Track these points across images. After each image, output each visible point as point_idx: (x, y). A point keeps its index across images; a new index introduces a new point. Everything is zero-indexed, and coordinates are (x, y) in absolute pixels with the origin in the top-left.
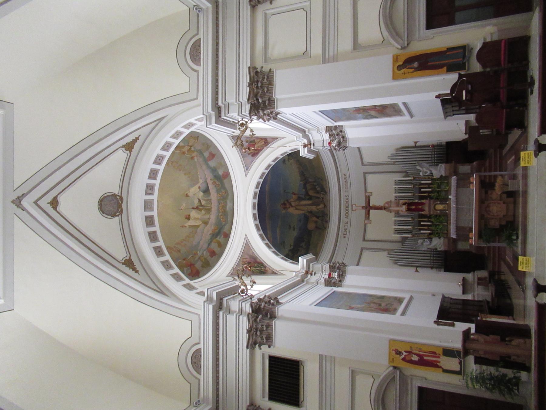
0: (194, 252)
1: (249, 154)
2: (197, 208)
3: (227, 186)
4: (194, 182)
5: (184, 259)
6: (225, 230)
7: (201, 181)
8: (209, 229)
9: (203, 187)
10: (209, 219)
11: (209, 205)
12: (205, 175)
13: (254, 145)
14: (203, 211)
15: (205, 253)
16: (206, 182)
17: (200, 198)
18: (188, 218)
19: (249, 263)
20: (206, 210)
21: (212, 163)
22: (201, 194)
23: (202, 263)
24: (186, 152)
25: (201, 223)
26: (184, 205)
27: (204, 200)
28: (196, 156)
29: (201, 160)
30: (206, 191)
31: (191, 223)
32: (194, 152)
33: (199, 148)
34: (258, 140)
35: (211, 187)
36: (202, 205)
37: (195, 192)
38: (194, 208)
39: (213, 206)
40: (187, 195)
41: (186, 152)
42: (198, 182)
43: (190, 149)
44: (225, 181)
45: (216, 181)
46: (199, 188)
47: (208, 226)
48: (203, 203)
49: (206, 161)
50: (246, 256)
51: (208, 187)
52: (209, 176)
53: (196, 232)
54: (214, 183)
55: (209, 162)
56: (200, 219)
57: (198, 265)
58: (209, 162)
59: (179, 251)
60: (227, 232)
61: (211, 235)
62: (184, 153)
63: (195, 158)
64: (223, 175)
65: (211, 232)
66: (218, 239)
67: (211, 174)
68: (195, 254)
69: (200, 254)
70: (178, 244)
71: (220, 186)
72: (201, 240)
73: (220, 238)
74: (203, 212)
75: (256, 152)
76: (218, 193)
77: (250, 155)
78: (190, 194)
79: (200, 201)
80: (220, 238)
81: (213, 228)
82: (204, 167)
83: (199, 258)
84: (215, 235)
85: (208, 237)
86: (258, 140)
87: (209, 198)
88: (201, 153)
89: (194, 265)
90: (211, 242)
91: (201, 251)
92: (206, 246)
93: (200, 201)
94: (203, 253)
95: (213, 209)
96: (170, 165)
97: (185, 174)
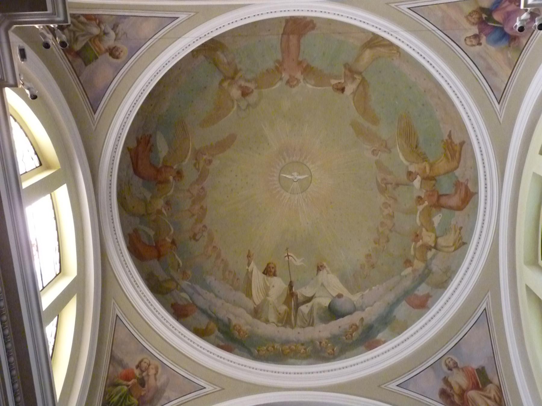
0: (189, 272)
1: (446, 381)
2: (291, 294)
3: (348, 353)
4: (354, 281)
5: (173, 242)
7: (356, 298)
8: (242, 320)
9: (342, 305)
10: (267, 321)
11: (299, 322)
12: (370, 303)
13: (476, 387)
14: (284, 308)
15: (184, 295)
16: (355, 309)
17: (315, 301)
18: (269, 271)
19: (142, 383)
20: (289, 315)
21: (402, 310)
22: (326, 302)
23: (161, 279)
24: (420, 243)
25: (258, 302)
28: (414, 271)
29: (407, 283)
30: (333, 313)
31: (258, 279)
32: (424, 260)
33: (436, 266)
34: (493, 394)
35: (344, 322)
36: (298, 305)
37: (328, 287)
38: (291, 286)
39: (298, 330)
40: (320, 268)
41: (420, 243)
42: (352, 291)
43: (429, 248)
44: (362, 348)
45: (360, 331)
46: (340, 296)
47: (249, 318)
48: (305, 309)
49: (406, 295)
50: (162, 379)
51: (343, 316)
52: (370, 314)
53: (236, 289)
55: (404, 303)
57: (154, 265)
58: (404, 303)
59: (194, 237)
61: (226, 320)
62: (417, 237)
63: (409, 270)
65: (234, 321)
66: (217, 332)
67: (374, 318)
68: (184, 273)
69: (184, 284)
70: (211, 239)
72: (216, 296)
73: (217, 337)
74: (283, 308)
75: (456, 399)
76: (328, 339)
77: (441, 385)
80: (217, 337)
81: (245, 328)
82: (391, 297)
83: (173, 279)
85: (222, 314)
86: (493, 394)
87: (315, 321)
88: (424, 276)
89: (159, 256)
90: (210, 317)
91: (190, 290)
92: (200, 302)
93: (309, 300)
94: (183, 290)
96: (386, 212)
97: (368, 256)
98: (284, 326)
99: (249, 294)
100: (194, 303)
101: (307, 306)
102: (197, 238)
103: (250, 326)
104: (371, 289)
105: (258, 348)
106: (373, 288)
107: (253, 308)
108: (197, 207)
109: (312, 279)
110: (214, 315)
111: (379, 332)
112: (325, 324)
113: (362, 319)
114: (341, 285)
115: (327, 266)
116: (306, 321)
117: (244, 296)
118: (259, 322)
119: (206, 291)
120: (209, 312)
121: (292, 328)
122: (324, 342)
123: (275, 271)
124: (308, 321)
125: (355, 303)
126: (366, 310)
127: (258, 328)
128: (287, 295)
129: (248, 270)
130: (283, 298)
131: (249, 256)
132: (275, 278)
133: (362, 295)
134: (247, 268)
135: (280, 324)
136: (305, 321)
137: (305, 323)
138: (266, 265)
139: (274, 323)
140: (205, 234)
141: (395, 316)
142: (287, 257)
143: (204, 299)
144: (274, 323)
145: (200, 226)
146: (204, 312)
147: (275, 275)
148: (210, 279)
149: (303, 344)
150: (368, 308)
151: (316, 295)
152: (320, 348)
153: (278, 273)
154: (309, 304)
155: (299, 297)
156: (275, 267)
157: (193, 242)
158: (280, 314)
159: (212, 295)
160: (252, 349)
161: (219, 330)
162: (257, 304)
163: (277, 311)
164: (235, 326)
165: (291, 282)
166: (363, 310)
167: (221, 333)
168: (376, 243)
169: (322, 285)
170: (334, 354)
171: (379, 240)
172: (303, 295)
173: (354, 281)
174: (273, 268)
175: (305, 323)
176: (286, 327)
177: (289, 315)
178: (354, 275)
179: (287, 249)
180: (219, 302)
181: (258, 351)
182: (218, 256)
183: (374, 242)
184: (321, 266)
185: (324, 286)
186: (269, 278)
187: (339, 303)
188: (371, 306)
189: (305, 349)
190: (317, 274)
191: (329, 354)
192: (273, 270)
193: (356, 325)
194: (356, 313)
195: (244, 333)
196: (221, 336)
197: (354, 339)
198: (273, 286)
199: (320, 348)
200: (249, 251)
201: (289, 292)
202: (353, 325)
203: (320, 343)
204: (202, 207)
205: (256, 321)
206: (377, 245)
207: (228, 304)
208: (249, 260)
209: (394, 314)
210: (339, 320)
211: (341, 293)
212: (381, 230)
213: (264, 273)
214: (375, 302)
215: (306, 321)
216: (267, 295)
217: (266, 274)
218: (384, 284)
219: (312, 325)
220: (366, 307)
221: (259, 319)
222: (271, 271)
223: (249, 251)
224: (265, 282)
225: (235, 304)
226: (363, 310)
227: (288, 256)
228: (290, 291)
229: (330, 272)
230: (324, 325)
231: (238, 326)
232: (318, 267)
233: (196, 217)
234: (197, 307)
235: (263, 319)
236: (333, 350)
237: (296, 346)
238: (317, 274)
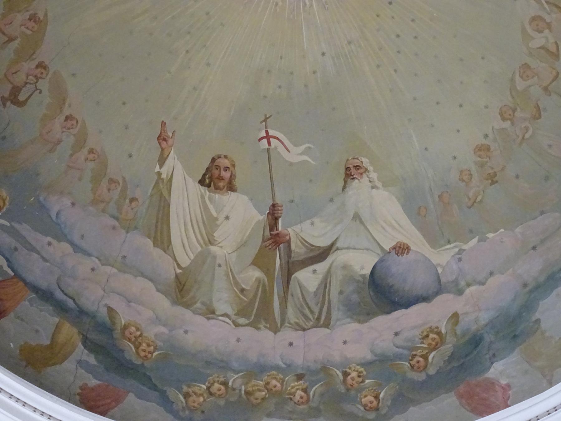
2: (275, 239)
4: (439, 210)
6: (131, 397)
7: (442, 258)
9: (407, 275)
10: (210, 313)
11: (292, 315)
14: (256, 274)
17: (337, 258)
18: (215, 178)
22: (363, 263)
25: (185, 261)
26: (295, 154)
27: (325, 284)
30: (382, 293)
31: (186, 197)
36: (290, 268)
37: (373, 224)
38: (274, 215)
39: (288, 334)
40: (351, 172)
42: (434, 243)
45: (447, 348)
46: (401, 249)
47: (164, 303)
48: (308, 278)
51: (407, 304)
52: (476, 306)
53: (129, 227)
54: (434, 337)
56: (203, 258)
60: (110, 413)
64: (491, 385)
66: (81, 352)
67: (485, 317)
70: (60, 97)
71: (421, 377)
72: (77, 248)
73: (80, 362)
76: (366, 364)
78: (359, 188)
79: (322, 254)
81: (152, 332)
82: (532, 268)
84: (104, 340)
85: (93, 298)
87: (336, 314)
90: (61, 308)
92: (36, 271)
93: (322, 254)
95: (266, 335)
96: (538, 41)
97: (482, 150)
98: (254, 325)
99: (163, 241)
100: (17, 276)
101: (315, 271)
102: (22, 98)
103: (165, 325)
104: (483, 240)
105: (185, 389)
106: (490, 235)
107: (173, 277)
108: (20, 18)
109: (331, 200)
110: (70, 303)
111: (494, 358)
112: (360, 322)
113: (455, 318)
114: (405, 221)
115: (371, 168)
116: (312, 312)
117: (150, 242)
118: (187, 314)
119: (49, 239)
120: (59, 295)
121: (276, 330)
122: (354, 374)
123: (232, 177)
124: (316, 310)
125: (440, 270)
126: (468, 291)
127: (186, 332)
128: (264, 241)
129: (159, 174)
130: (252, 251)
131: (162, 138)
132: (232, 195)
133: (461, 251)
134: (157, 169)
135: (242, 321)
136: (307, 312)
137: (305, 316)
138: (207, 164)
139: (225, 315)
140: (43, 85)
141: (538, 321)
142: (265, 141)
143: (46, 260)
144: (225, 315)
145: (28, 66)
146: (45, 295)
147: (231, 188)
148: (57, 204)
149: (300, 377)
150: (473, 288)
151: (338, 244)
152: (342, 389)
153: (237, 182)
154: (321, 267)
155: (293, 247)
156: (234, 166)
157: (12, 109)
158: (242, 290)
159: (66, 247)
160: (172, 392)
161: (85, 341)
162: (183, 266)
163: (237, 284)
164: (126, 327)
165: (274, 205)
166: (460, 292)
167: (91, 351)
168: (504, 119)
169: (357, 217)
170: (377, 409)
171: (514, 111)
172: (304, 242)
173: (439, 210)
174: (226, 169)
175: (305, 316)
176: (258, 329)
177: (266, 303)
178: (440, 196)
179: (265, 120)
180: (83, 266)
181: (187, 396)
182: (80, 142)
183: (501, 115)
184: (357, 167)
185: (362, 222)
186: (217, 196)
187: (398, 265)
188: (483, 284)
189: (305, 391)
190: (344, 188)
191: (365, 406)
192: (226, 175)
193: (439, 333)
194: (439, 298)
195: (149, 345)
196: (92, 360)
197: (432, 371)
198: (227, 218)
199: (342, 389)
200: (163, 124)
201: (267, 233)
202: (431, 330)
203: (346, 374)
204: (33, 18)
205: (180, 310)
206: (507, 124)
207: (108, 269)
208: (163, 149)
209: (537, 315)
210: (396, 314)
211: (406, 241)
212: (520, 85)
213: (202, 182)
214: (491, 274)
215: (312, 312)
216: (211, 242)
217: (209, 186)
218: (518, 230)
219: (327, 325)
220: (468, 285)
221: (187, 306)
222: (220, 178)
223: (163, 124)
224: (204, 202)
225: (125, 266)
226: (460, 292)
227: (268, 137)
228: (271, 230)
229: (379, 184)
230: (355, 326)
231: (133, 329)
232: (347, 169)
233: (15, 44)
234: (26, 283)
235: (198, 305)
236: (377, 397)
237: (282, 381)
238: (344, 188)
